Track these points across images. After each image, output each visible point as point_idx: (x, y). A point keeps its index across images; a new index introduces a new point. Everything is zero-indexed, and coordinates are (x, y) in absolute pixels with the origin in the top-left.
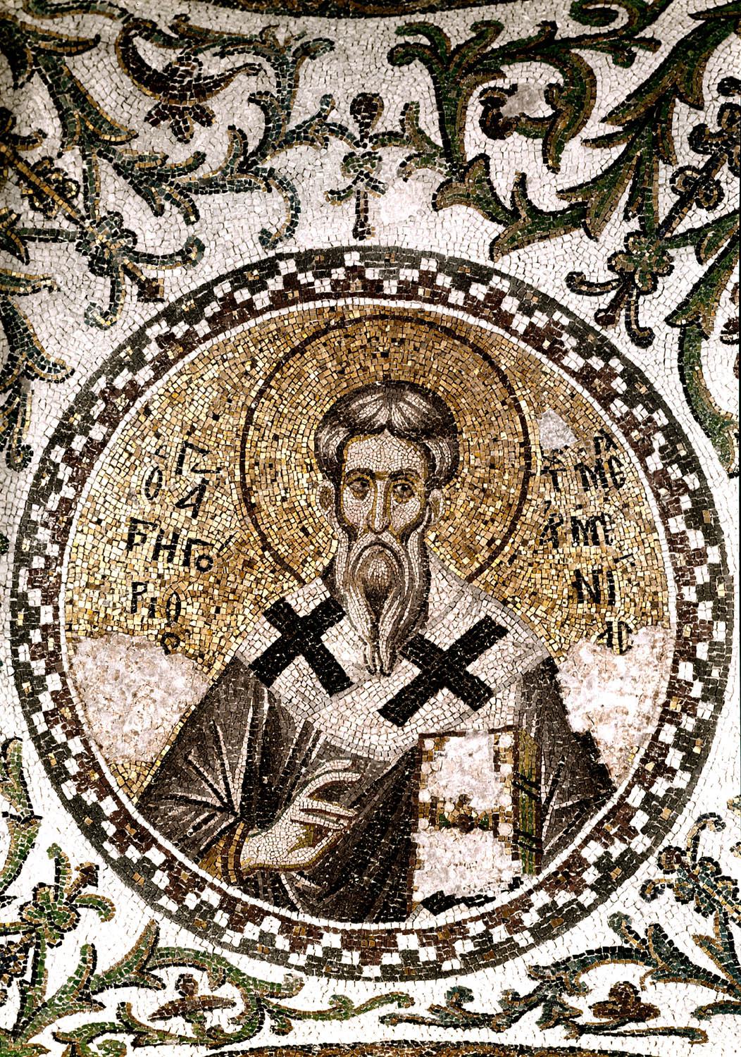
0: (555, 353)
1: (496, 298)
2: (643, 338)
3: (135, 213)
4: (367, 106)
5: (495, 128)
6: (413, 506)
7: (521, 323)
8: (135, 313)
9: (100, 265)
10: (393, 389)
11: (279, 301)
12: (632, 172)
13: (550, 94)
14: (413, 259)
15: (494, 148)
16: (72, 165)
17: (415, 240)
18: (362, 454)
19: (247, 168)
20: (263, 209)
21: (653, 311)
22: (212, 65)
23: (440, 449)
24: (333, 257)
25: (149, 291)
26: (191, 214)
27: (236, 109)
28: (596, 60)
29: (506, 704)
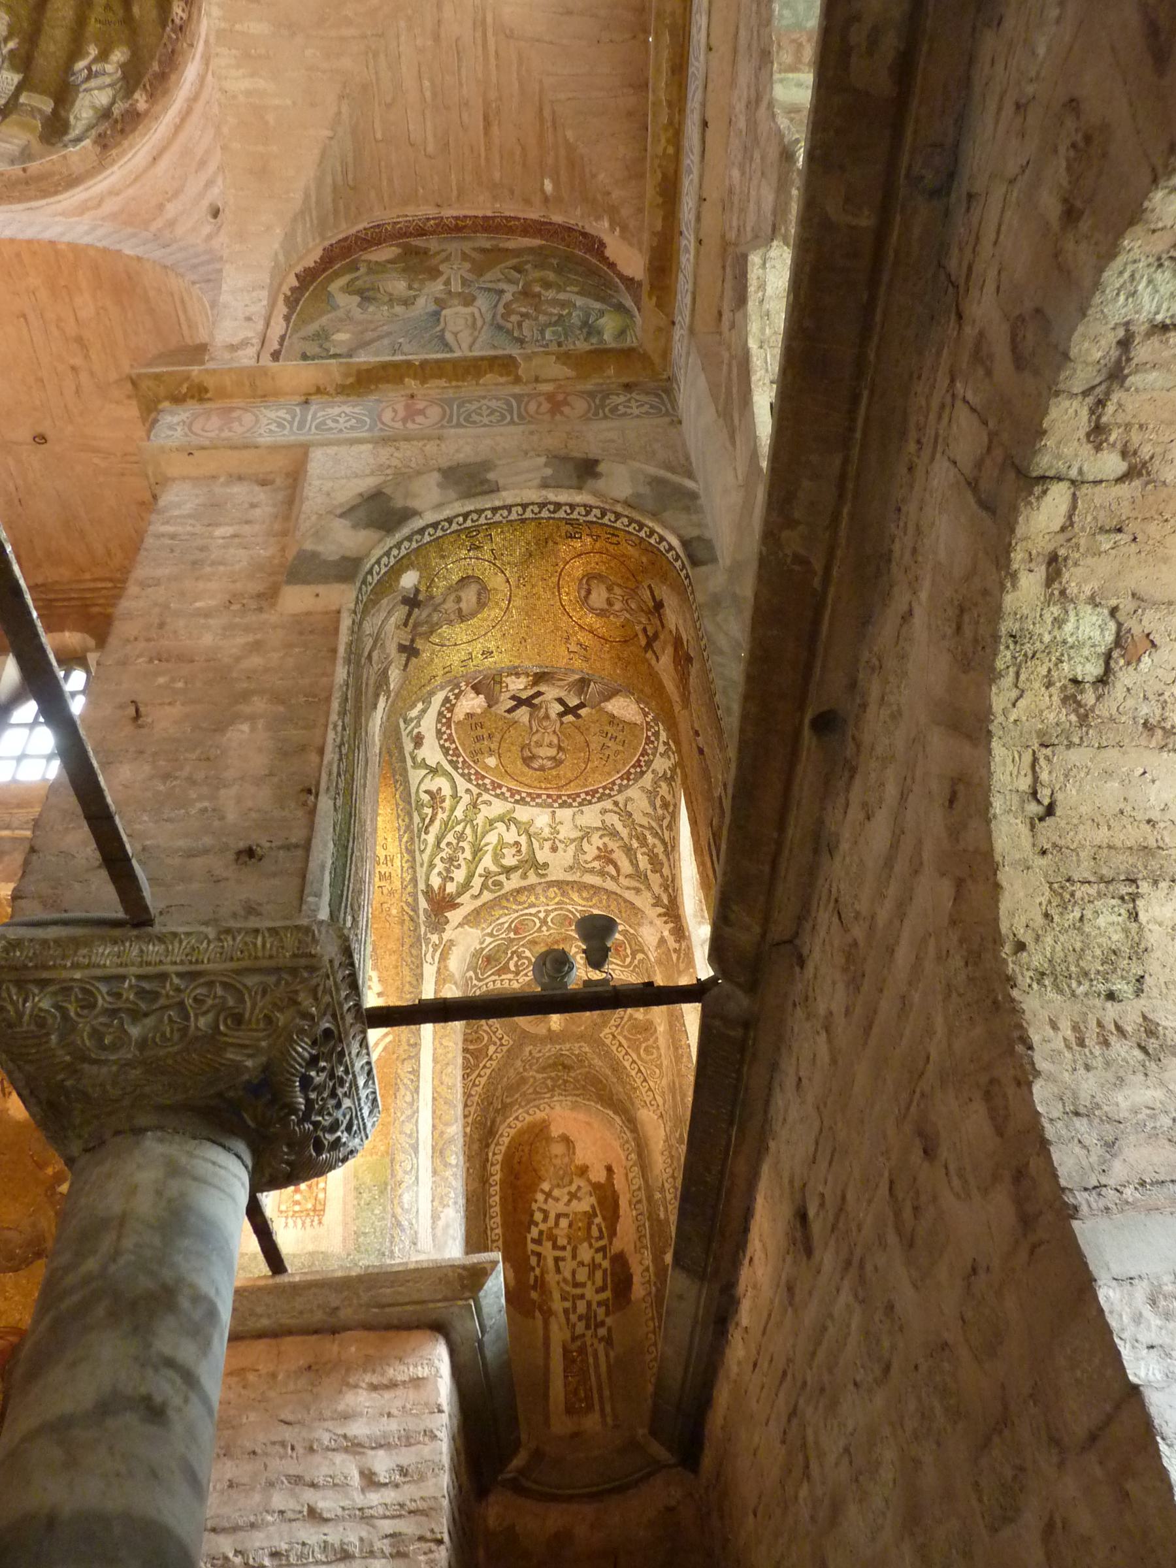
0: (493, 782)
1: (512, 796)
2: (468, 791)
3: (619, 827)
4: (554, 849)
5: (517, 843)
6: (535, 738)
7: (504, 790)
8: (620, 799)
9: (630, 815)
10: (542, 769)
11: (578, 795)
12: (478, 837)
13: (503, 856)
14: (538, 805)
15: (518, 839)
16: (635, 844)
17: (537, 810)
18: (552, 752)
19: (586, 834)
20: (583, 821)
21: (466, 799)
22: (596, 864)
23: (527, 753)
24: (561, 806)
25: (616, 803)
26: (603, 822)
27: (591, 851)
28: (494, 868)
29: (504, 696)
